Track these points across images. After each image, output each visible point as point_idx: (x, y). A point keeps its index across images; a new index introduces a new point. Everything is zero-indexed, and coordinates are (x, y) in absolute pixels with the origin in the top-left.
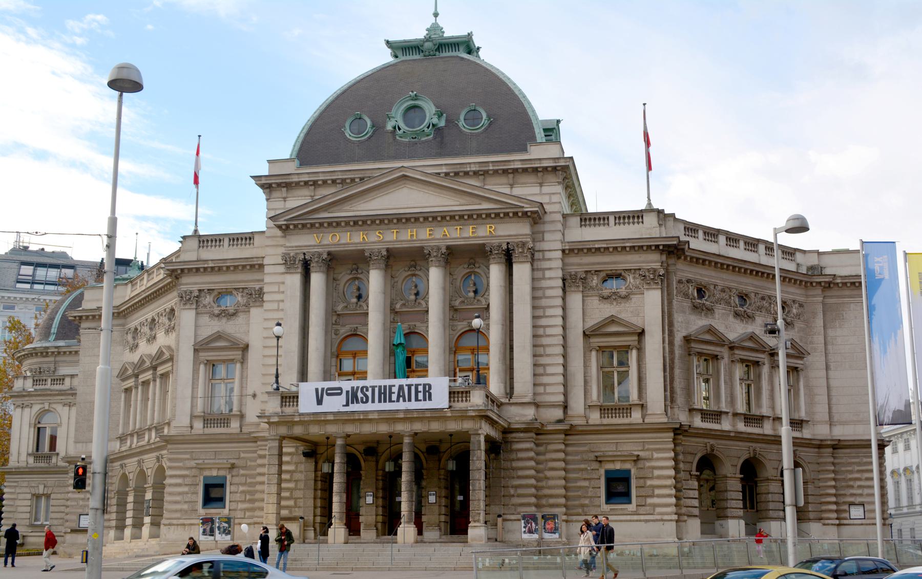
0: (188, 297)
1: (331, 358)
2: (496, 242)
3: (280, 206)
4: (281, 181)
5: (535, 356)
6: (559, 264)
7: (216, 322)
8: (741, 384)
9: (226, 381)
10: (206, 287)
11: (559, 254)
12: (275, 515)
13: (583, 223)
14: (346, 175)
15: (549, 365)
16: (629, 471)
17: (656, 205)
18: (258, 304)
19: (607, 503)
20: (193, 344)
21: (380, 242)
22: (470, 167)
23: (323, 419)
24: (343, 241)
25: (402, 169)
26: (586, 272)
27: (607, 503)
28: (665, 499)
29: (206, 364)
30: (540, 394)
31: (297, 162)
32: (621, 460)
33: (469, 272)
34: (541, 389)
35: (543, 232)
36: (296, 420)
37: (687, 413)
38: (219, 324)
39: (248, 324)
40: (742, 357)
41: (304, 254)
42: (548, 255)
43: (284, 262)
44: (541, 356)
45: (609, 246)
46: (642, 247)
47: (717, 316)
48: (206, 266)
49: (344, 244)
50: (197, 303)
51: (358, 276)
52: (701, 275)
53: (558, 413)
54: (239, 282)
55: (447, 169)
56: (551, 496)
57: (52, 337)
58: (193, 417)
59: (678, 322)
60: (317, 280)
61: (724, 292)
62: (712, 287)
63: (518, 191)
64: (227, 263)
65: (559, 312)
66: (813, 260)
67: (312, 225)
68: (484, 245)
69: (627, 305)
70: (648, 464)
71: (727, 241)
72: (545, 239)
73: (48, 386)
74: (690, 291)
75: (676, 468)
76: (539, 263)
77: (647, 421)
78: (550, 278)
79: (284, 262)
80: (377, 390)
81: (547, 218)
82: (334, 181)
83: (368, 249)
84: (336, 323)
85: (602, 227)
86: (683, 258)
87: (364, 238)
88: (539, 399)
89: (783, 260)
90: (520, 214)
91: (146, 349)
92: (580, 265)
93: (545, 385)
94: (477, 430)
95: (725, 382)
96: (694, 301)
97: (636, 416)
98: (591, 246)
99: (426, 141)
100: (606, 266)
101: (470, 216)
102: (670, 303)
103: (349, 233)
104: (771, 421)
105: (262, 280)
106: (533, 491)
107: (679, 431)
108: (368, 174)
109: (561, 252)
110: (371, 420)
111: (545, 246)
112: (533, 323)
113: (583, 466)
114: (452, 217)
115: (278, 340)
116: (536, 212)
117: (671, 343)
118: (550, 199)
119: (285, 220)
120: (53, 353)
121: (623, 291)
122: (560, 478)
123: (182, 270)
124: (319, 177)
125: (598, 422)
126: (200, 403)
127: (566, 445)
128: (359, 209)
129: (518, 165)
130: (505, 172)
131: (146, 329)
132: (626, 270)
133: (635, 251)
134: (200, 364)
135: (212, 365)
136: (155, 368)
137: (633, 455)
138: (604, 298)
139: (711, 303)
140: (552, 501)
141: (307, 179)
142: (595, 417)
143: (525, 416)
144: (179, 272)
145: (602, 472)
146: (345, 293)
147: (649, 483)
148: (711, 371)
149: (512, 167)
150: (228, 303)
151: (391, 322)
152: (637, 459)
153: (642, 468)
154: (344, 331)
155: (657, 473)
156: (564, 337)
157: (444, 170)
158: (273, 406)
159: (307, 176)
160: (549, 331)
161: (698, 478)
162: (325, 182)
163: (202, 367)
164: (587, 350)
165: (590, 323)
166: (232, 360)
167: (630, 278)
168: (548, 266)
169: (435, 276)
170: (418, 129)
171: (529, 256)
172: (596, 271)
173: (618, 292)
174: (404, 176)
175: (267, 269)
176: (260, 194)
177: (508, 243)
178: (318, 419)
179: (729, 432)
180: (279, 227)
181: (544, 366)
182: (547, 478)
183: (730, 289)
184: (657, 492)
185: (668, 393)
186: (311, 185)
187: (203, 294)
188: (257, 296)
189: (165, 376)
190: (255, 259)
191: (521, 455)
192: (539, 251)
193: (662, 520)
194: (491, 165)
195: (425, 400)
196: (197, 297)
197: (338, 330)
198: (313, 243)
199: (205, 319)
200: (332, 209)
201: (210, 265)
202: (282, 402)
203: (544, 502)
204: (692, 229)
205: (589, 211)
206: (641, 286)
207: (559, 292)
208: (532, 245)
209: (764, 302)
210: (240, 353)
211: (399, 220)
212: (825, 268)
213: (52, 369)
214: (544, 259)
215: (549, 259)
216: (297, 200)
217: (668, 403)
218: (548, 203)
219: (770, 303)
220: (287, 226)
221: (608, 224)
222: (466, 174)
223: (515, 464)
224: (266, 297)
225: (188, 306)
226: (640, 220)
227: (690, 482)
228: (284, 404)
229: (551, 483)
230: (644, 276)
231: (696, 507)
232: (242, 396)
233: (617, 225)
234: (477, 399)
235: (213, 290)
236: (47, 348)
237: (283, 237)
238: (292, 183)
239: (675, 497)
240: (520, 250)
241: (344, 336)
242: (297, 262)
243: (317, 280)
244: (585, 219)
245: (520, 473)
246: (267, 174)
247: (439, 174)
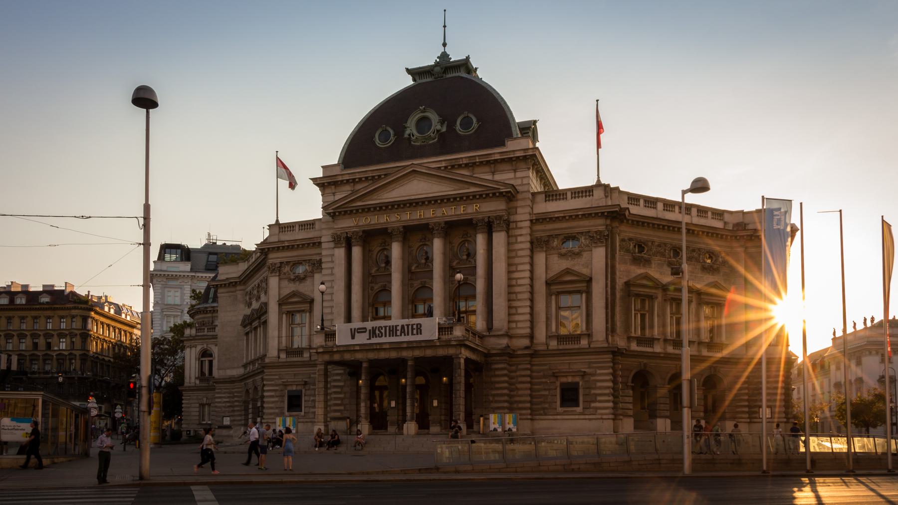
0: (273, 268)
1: (369, 307)
2: (480, 216)
3: (331, 199)
4: (330, 181)
5: (509, 300)
6: (526, 231)
7: (292, 284)
8: (671, 317)
9: (301, 325)
11: (528, 224)
12: (323, 416)
13: (547, 199)
15: (519, 307)
16: (578, 383)
18: (319, 271)
19: (562, 406)
20: (277, 300)
21: (398, 221)
22: (462, 161)
23: (352, 349)
24: (373, 222)
27: (562, 406)
28: (605, 404)
29: (286, 314)
30: (513, 328)
31: (342, 166)
32: (572, 376)
33: (463, 241)
34: (514, 325)
35: (516, 208)
36: (334, 350)
37: (626, 340)
38: (295, 286)
39: (313, 285)
40: (673, 296)
41: (347, 233)
42: (520, 225)
43: (333, 239)
44: (514, 300)
45: (565, 215)
46: (591, 214)
47: (653, 265)
48: (283, 245)
49: (374, 224)
50: (279, 272)
51: (386, 247)
52: (640, 234)
53: (526, 342)
55: (445, 164)
56: (521, 402)
57: (211, 300)
59: (620, 271)
60: (357, 251)
61: (660, 247)
62: (650, 244)
63: (498, 177)
65: (528, 267)
66: (739, 219)
67: (351, 211)
68: (471, 219)
69: (579, 260)
70: (592, 378)
71: (664, 207)
72: (518, 212)
73: (206, 333)
74: (631, 247)
75: (615, 382)
76: (513, 231)
77: (592, 346)
78: (521, 242)
79: (333, 239)
80: (388, 328)
81: (519, 196)
82: (367, 178)
83: (391, 227)
84: (372, 282)
85: (562, 201)
86: (625, 221)
87: (387, 219)
88: (512, 332)
89: (712, 220)
90: (497, 194)
91: (255, 305)
92: (543, 231)
93: (516, 322)
94: (458, 355)
95: (658, 316)
96: (634, 255)
97: (584, 342)
98: (552, 216)
99: (433, 143)
100: (563, 231)
101: (461, 198)
102: (613, 257)
103: (376, 217)
104: (696, 345)
105: (321, 254)
106: (506, 398)
107: (616, 353)
108: (390, 171)
109: (529, 222)
110: (385, 349)
111: (518, 218)
112: (508, 277)
113: (544, 380)
114: (448, 200)
115: (322, 294)
116: (510, 192)
117: (613, 288)
118: (522, 181)
120: (210, 311)
121: (577, 250)
122: (526, 389)
124: (356, 176)
125: (555, 348)
126: (284, 340)
127: (532, 365)
128: (383, 197)
129: (498, 157)
130: (488, 163)
131: (255, 292)
132: (580, 233)
133: (586, 218)
134: (283, 314)
135: (291, 314)
136: (259, 318)
137: (582, 371)
138: (562, 256)
139: (649, 255)
140: (521, 405)
141: (348, 178)
142: (553, 344)
143: (501, 344)
144: (266, 250)
145: (558, 384)
146: (378, 261)
147: (593, 392)
148: (647, 308)
149: (493, 158)
150: (300, 270)
151: (409, 280)
152: (584, 374)
153: (587, 381)
154: (377, 287)
155: (599, 384)
156: (532, 286)
157: (444, 164)
158: (319, 341)
159: (347, 176)
160: (520, 282)
161: (633, 388)
162: (360, 179)
163: (284, 316)
164: (549, 295)
165: (552, 274)
166: (303, 311)
167: (583, 240)
168: (520, 233)
169: (437, 244)
170: (427, 134)
171: (505, 226)
173: (573, 251)
174: (414, 171)
175: (324, 246)
176: (317, 192)
177: (489, 217)
178: (348, 349)
179: (660, 353)
180: (329, 214)
181: (516, 308)
182: (517, 389)
183: (665, 244)
184: (599, 398)
185: (609, 325)
186: (351, 182)
187: (283, 265)
188: (317, 265)
189: (265, 323)
190: (315, 239)
191: (497, 373)
192: (514, 222)
193: (602, 419)
194: (477, 158)
195: (417, 334)
196: (280, 267)
197: (373, 287)
198: (352, 225)
199: (285, 283)
200: (365, 199)
201: (286, 245)
202: (326, 338)
203: (515, 406)
204: (634, 198)
205: (560, 188)
206: (589, 245)
207: (528, 252)
208: (506, 218)
209: (694, 254)
210: (308, 305)
211: (411, 204)
212: (748, 224)
213: (211, 322)
214: (517, 228)
215: (521, 228)
216: (341, 194)
217: (609, 332)
218: (520, 185)
219: (700, 255)
220: (334, 213)
221: (566, 198)
222: (460, 166)
223: (493, 379)
224: (324, 266)
225: (273, 274)
226: (591, 194)
227: (627, 391)
228: (327, 339)
229: (520, 392)
230: (593, 237)
231: (630, 409)
232: (310, 335)
233: (573, 199)
234: (458, 332)
235: (290, 262)
236: (206, 308)
237: (334, 222)
238: (338, 181)
239: (613, 402)
240: (498, 222)
241: (377, 291)
242: (342, 239)
243: (357, 251)
244: (549, 196)
245: (497, 385)
246: (321, 176)
247: (440, 168)
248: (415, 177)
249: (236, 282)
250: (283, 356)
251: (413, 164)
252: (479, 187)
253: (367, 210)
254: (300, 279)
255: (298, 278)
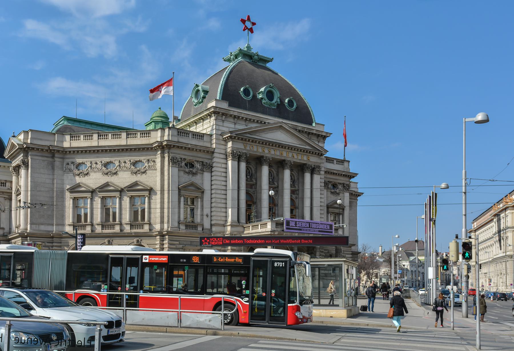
10: (183, 157)
11: (324, 172)
14: (253, 117)
17: (346, 159)
25: (282, 123)
26: (329, 181)
38: (188, 177)
48: (187, 146)
54: (200, 157)
58: (179, 223)
64: (197, 147)
68: (306, 164)
119: (235, 134)
123: (174, 146)
124: (241, 115)
159: (237, 113)
172: (331, 182)
175: (215, 155)
199: (182, 173)
201: (189, 147)
220: (235, 137)
238: (228, 114)
243: (243, 165)
248: (279, 129)
249: (58, 151)
250: (183, 227)
251: (282, 122)
252: (309, 146)
253: (254, 141)
254: (194, 174)
255: (192, 172)
